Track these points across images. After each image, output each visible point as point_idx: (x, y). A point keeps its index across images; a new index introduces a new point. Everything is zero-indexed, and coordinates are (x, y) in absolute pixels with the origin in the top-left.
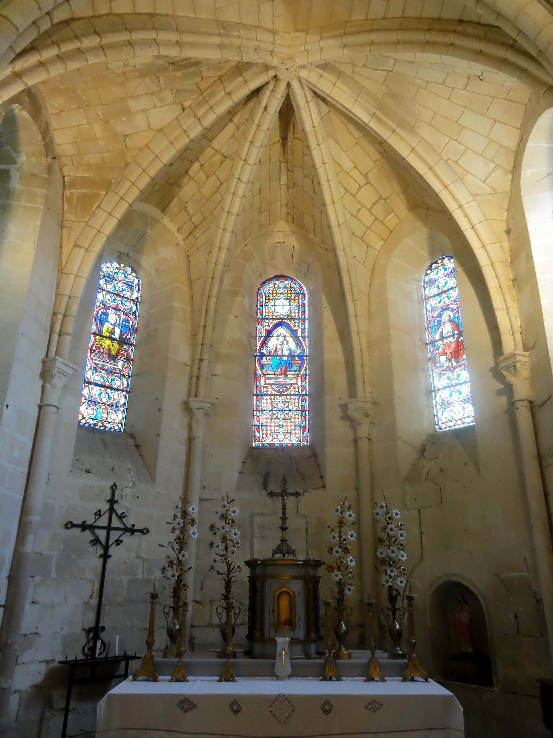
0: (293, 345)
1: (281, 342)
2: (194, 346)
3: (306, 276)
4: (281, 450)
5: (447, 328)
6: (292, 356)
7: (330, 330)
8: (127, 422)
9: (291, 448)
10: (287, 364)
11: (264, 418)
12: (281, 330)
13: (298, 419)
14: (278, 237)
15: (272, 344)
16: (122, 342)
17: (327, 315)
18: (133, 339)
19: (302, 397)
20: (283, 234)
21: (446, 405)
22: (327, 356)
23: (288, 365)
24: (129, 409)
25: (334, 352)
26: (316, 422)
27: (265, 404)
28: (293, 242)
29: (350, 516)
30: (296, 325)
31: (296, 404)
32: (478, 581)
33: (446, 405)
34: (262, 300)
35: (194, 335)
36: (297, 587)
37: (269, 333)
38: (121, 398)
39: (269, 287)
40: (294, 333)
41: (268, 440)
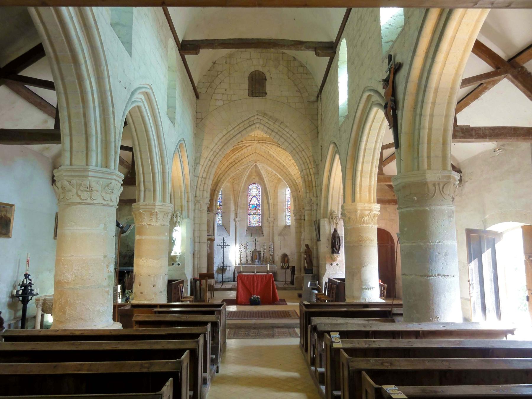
0: (257, 202)
1: (254, 201)
2: (235, 206)
3: (260, 184)
4: (255, 227)
5: (290, 202)
6: (257, 205)
7: (265, 202)
8: (222, 223)
9: (257, 227)
10: (256, 206)
11: (251, 220)
12: (254, 198)
13: (258, 219)
14: (254, 177)
15: (252, 202)
16: (219, 205)
17: (265, 197)
18: (221, 204)
19: (259, 215)
20: (255, 177)
21: (289, 219)
22: (265, 207)
23: (256, 207)
24: (222, 220)
25: (266, 207)
26: (262, 221)
27: (251, 217)
28: (257, 178)
29: (265, 244)
30: (258, 197)
31: (258, 217)
32: (288, 253)
33: (289, 219)
34: (250, 190)
35: (235, 204)
36: (257, 254)
37: (251, 199)
38: (220, 218)
39: (251, 187)
40: (257, 199)
41: (252, 225)
